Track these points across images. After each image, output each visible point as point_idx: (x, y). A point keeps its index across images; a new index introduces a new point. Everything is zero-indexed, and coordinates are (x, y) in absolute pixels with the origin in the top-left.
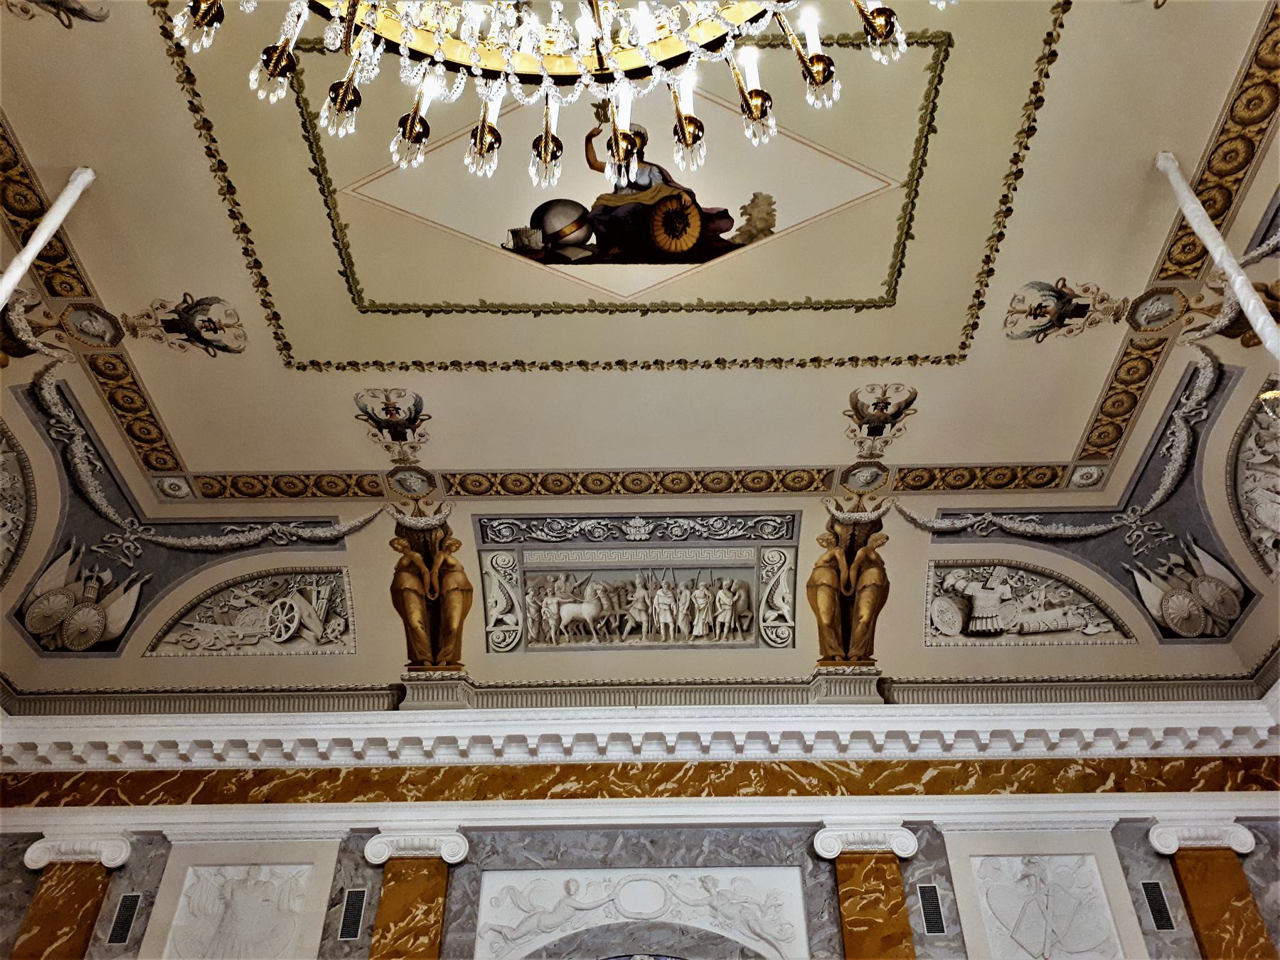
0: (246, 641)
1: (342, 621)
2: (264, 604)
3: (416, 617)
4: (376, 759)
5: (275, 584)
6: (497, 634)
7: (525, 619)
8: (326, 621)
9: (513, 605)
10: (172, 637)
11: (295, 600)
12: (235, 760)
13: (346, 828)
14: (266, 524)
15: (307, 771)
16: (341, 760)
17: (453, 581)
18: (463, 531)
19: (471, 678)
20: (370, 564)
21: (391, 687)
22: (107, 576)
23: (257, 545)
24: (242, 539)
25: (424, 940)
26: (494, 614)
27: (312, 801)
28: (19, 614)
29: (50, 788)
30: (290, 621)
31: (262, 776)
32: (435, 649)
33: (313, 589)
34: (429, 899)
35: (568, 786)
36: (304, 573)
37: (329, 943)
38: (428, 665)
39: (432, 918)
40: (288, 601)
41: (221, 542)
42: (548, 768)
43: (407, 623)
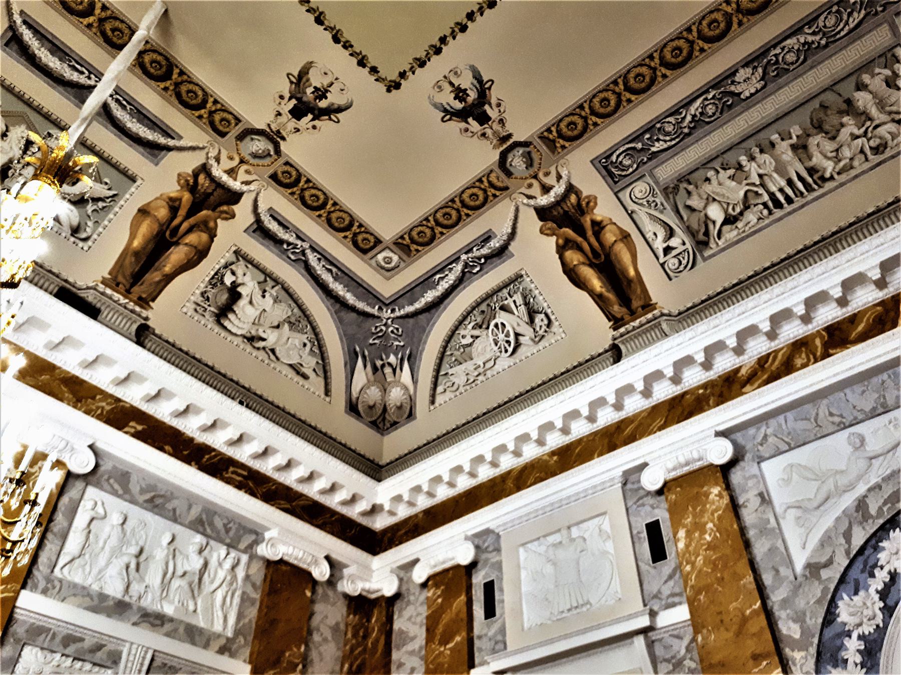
0: (488, 365)
1: (543, 316)
3: (597, 284)
5: (483, 312)
6: (672, 263)
8: (532, 321)
9: (671, 229)
10: (440, 389)
11: (502, 317)
13: (619, 472)
17: (610, 236)
18: (591, 184)
26: (659, 245)
30: (508, 335)
32: (625, 301)
33: (510, 302)
38: (627, 317)
40: (498, 320)
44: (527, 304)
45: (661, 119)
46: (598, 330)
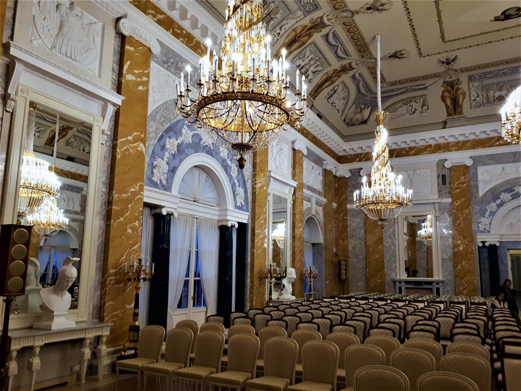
2: (405, 106)
3: (449, 102)
4: (441, 141)
7: (483, 98)
8: (422, 107)
11: (413, 103)
12: (403, 146)
14: (405, 88)
15: (423, 146)
16: (432, 142)
17: (459, 92)
19: (466, 116)
20: (435, 91)
21: (442, 122)
22: (363, 106)
23: (403, 93)
24: (399, 92)
25: (465, 185)
26: (472, 99)
27: (427, 154)
28: (345, 120)
29: (359, 157)
31: (411, 149)
32: (455, 110)
34: (464, 175)
35: (500, 142)
36: (415, 97)
37: (440, 187)
38: (453, 114)
39: (466, 180)
41: (393, 94)
42: (494, 138)
43: (446, 105)
44: (423, 102)
45: (494, 71)
46: (443, 115)
